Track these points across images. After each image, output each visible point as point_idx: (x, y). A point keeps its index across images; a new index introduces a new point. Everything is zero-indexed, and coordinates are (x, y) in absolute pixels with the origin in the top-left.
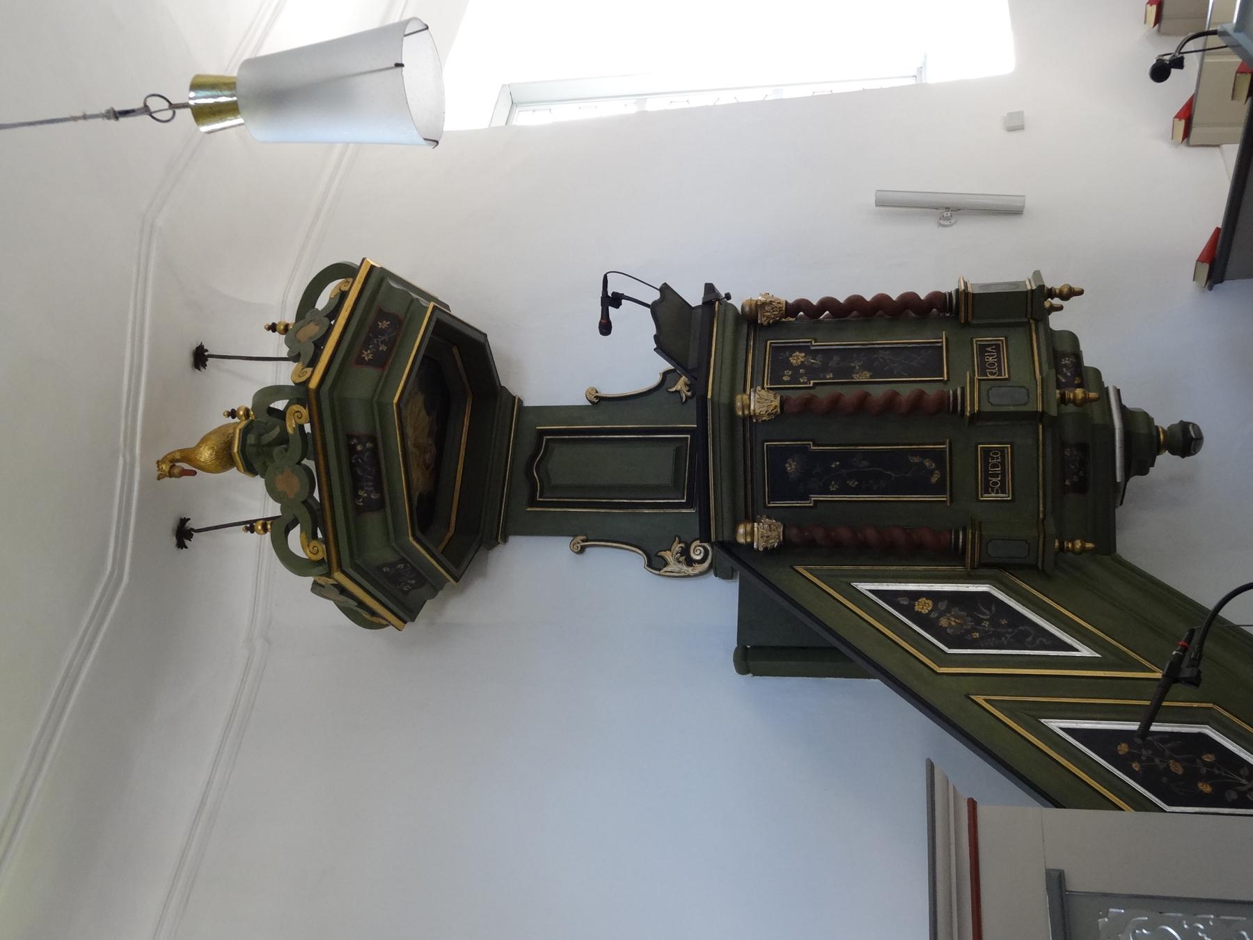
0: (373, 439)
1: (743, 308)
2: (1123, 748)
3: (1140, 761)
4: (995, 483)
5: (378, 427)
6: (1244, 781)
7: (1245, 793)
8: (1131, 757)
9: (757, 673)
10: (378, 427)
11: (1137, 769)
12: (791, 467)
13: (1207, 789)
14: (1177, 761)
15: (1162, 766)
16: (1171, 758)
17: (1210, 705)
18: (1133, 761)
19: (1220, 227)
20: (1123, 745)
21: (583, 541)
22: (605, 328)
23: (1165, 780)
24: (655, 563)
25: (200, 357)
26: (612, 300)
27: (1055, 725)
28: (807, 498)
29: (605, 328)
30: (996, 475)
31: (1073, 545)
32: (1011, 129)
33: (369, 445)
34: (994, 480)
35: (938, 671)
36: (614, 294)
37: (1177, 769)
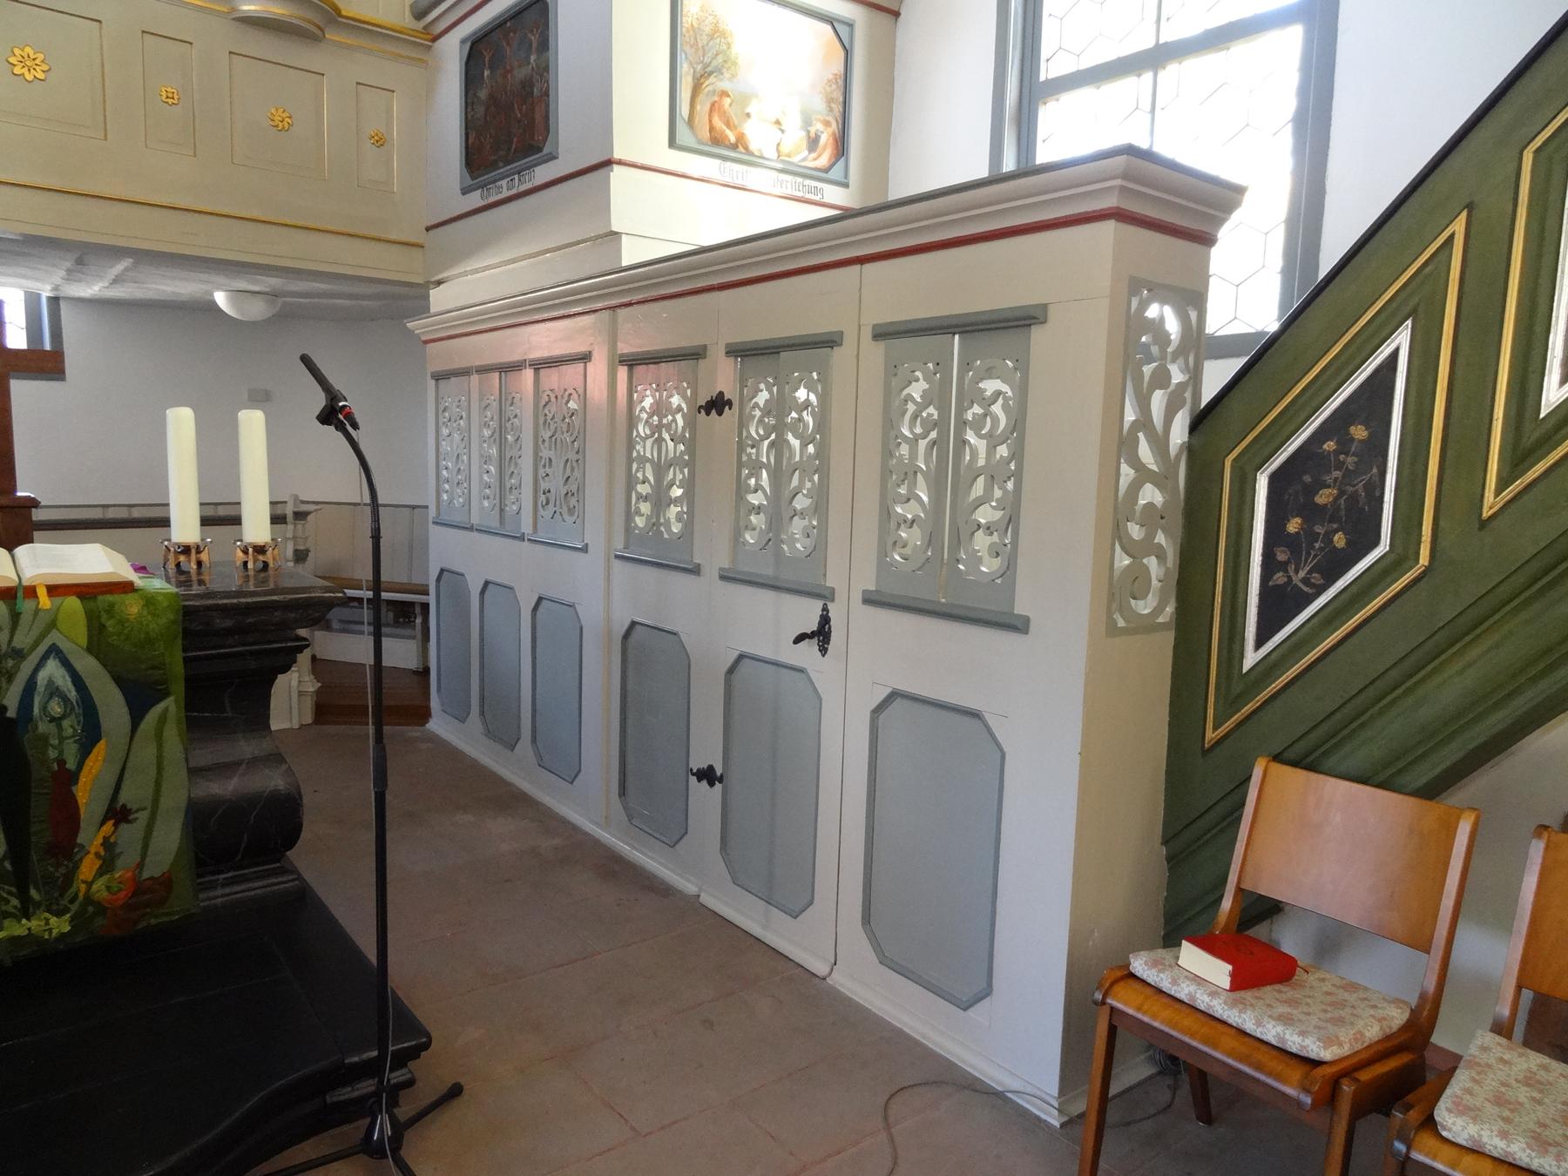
2: (1359, 432)
3: (1337, 452)
6: (1302, 574)
7: (1286, 571)
8: (1345, 443)
11: (1325, 446)
13: (1293, 526)
14: (1336, 499)
15: (1328, 479)
16: (1342, 493)
17: (1424, 559)
18: (1338, 443)
20: (1365, 434)
23: (1307, 479)
27: (1402, 339)
35: (1525, 152)
37: (1324, 497)
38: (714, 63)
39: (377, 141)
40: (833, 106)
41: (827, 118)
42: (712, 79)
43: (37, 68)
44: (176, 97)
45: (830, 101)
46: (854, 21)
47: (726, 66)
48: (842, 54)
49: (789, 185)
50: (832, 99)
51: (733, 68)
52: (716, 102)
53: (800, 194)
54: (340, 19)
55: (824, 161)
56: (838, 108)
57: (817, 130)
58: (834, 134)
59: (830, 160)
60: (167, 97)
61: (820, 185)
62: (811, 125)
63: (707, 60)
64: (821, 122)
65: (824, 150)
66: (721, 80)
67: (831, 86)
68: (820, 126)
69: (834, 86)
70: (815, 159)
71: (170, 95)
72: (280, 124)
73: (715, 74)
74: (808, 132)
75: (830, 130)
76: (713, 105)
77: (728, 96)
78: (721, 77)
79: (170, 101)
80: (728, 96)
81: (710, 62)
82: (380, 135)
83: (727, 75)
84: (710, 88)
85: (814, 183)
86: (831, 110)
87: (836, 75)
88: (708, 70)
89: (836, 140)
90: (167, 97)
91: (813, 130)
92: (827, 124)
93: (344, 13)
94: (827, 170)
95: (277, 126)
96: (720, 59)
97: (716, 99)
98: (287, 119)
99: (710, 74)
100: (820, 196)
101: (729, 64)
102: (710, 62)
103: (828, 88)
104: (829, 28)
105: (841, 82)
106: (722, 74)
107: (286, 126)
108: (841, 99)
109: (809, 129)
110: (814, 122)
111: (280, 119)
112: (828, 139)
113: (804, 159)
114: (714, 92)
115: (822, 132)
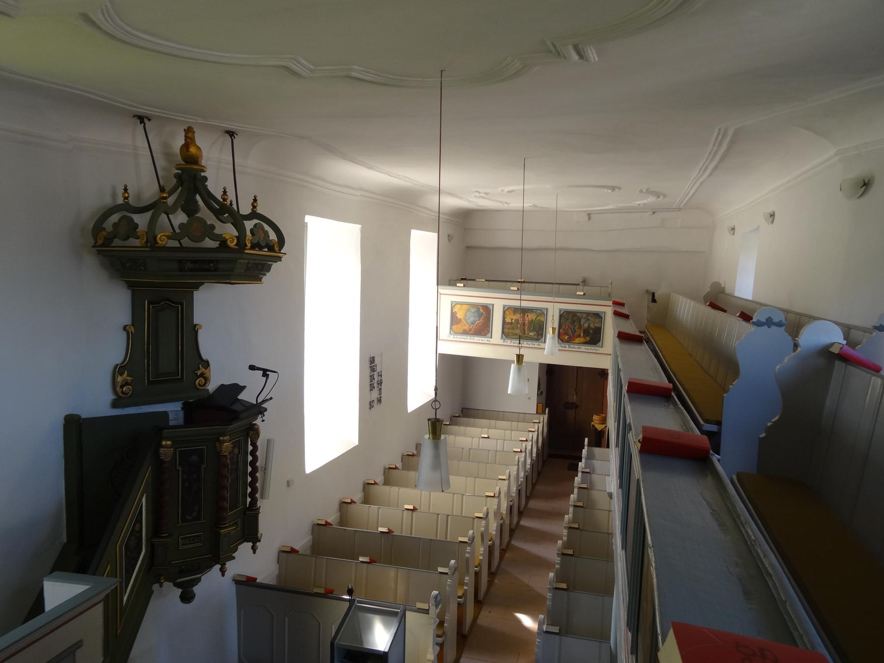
0: (216, 270)
1: (255, 424)
4: (186, 541)
5: (220, 273)
9: (65, 426)
10: (220, 273)
12: (194, 458)
19: (258, 581)
21: (131, 332)
22: (252, 368)
24: (119, 370)
25: (231, 134)
26: (265, 373)
28: (180, 465)
29: (252, 368)
30: (189, 541)
31: (162, 579)
32: (288, 482)
33: (213, 269)
34: (187, 540)
36: (268, 375)
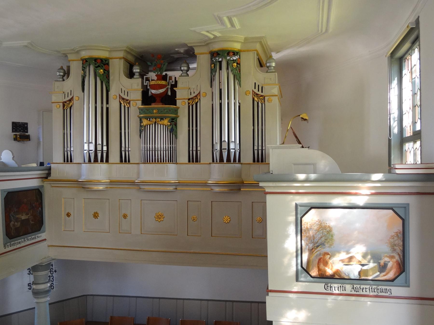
38: (320, 242)
39: (259, 221)
40: (395, 248)
41: (392, 254)
42: (319, 249)
43: (161, 218)
44: (196, 218)
45: (393, 247)
46: (408, 204)
47: (327, 241)
48: (400, 221)
49: (368, 290)
50: (395, 245)
51: (331, 241)
52: (321, 258)
53: (375, 294)
54: (244, 184)
55: (391, 275)
56: (399, 249)
57: (386, 261)
58: (397, 261)
59: (394, 275)
60: (193, 219)
61: (388, 288)
62: (381, 259)
63: (316, 240)
64: (387, 257)
65: (390, 270)
66: (324, 248)
67: (393, 238)
68: (387, 259)
69: (396, 238)
70: (384, 276)
71: (195, 218)
72: (227, 221)
73: (320, 246)
74: (379, 263)
75: (394, 260)
76: (320, 260)
77: (329, 254)
78: (324, 247)
79: (194, 220)
80: (329, 254)
81: (318, 242)
82: (260, 219)
83: (327, 245)
84: (318, 253)
85: (386, 287)
86: (394, 250)
87: (398, 232)
88: (317, 245)
89: (398, 264)
90: (193, 219)
91: (382, 262)
92: (392, 257)
93: (245, 182)
94: (393, 280)
95: (225, 222)
96: (323, 239)
97: (322, 257)
98: (229, 219)
99: (318, 247)
100: (390, 293)
101: (329, 240)
102: (318, 242)
103: (392, 240)
104: (391, 211)
105: (401, 236)
106: (324, 245)
107: (228, 221)
108: (401, 243)
109: (379, 261)
110: (383, 258)
111: (227, 219)
112: (393, 265)
113: (378, 276)
114: (320, 254)
115: (390, 262)
